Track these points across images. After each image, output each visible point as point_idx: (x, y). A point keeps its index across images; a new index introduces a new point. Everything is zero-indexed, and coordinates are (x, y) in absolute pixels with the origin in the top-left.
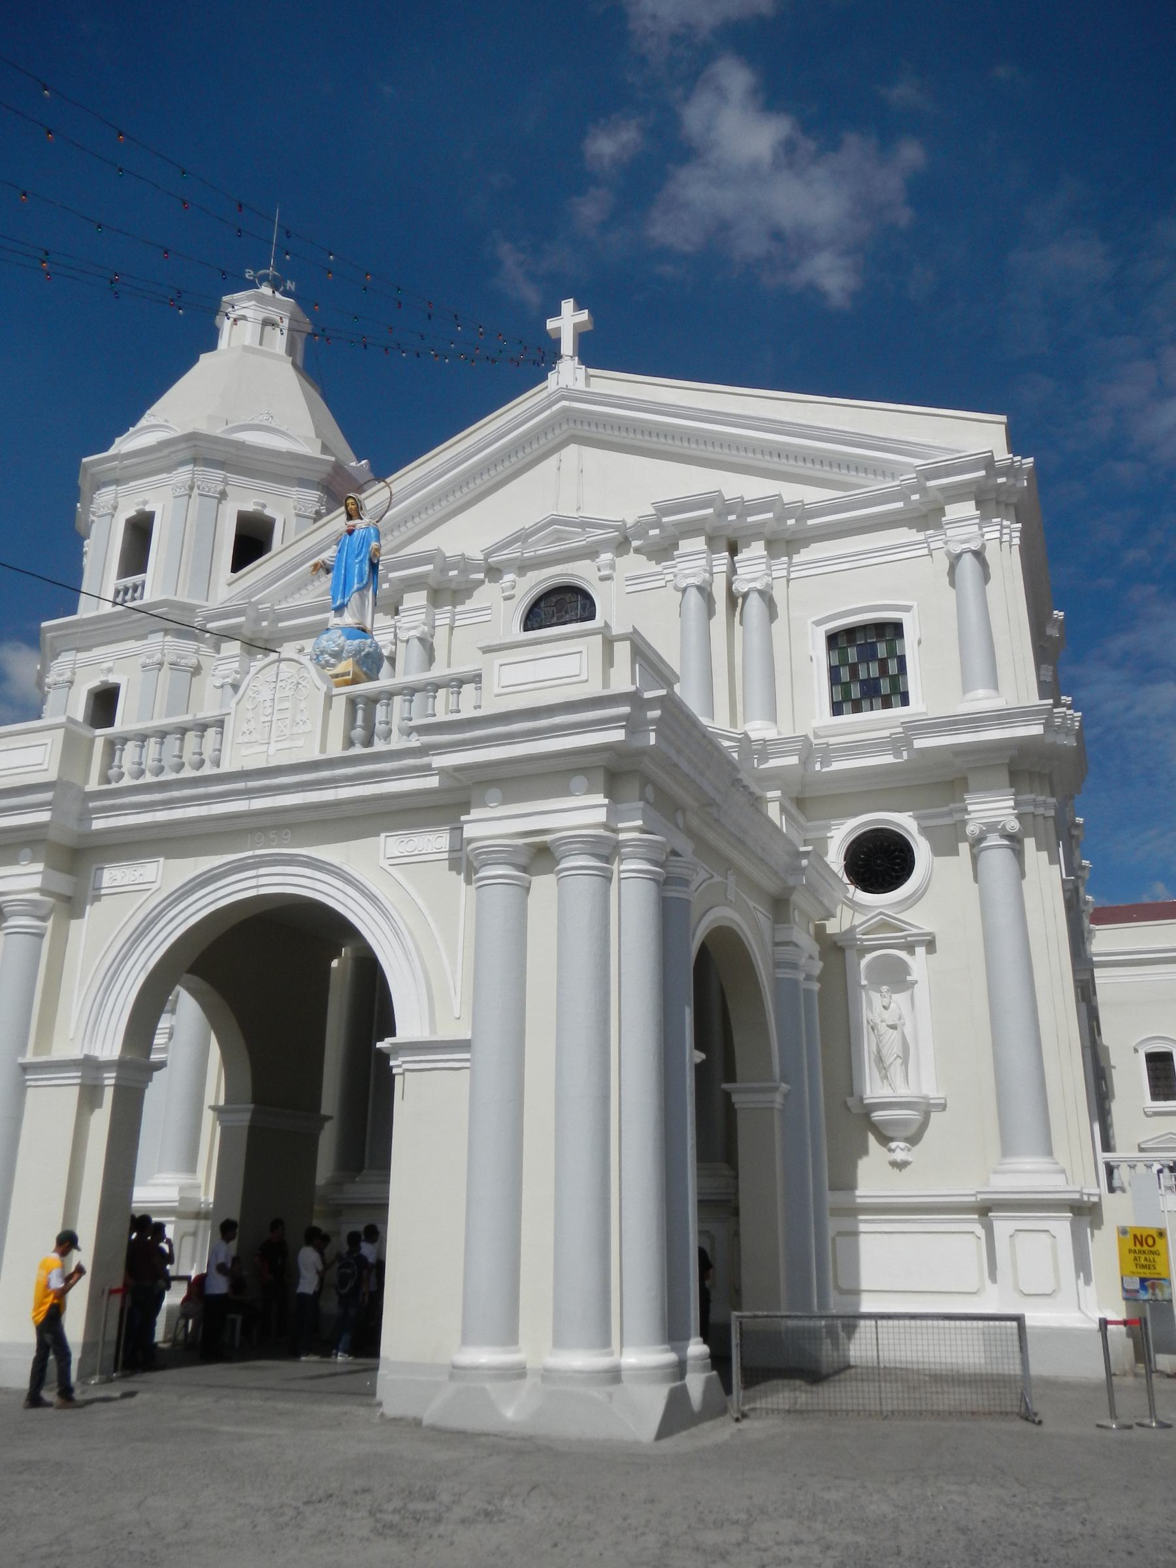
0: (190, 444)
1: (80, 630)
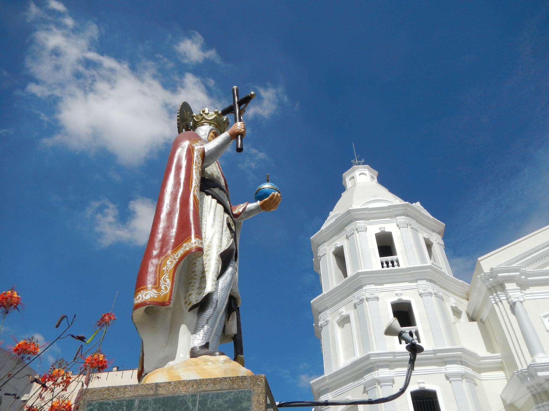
0: (404, 208)
1: (378, 275)
